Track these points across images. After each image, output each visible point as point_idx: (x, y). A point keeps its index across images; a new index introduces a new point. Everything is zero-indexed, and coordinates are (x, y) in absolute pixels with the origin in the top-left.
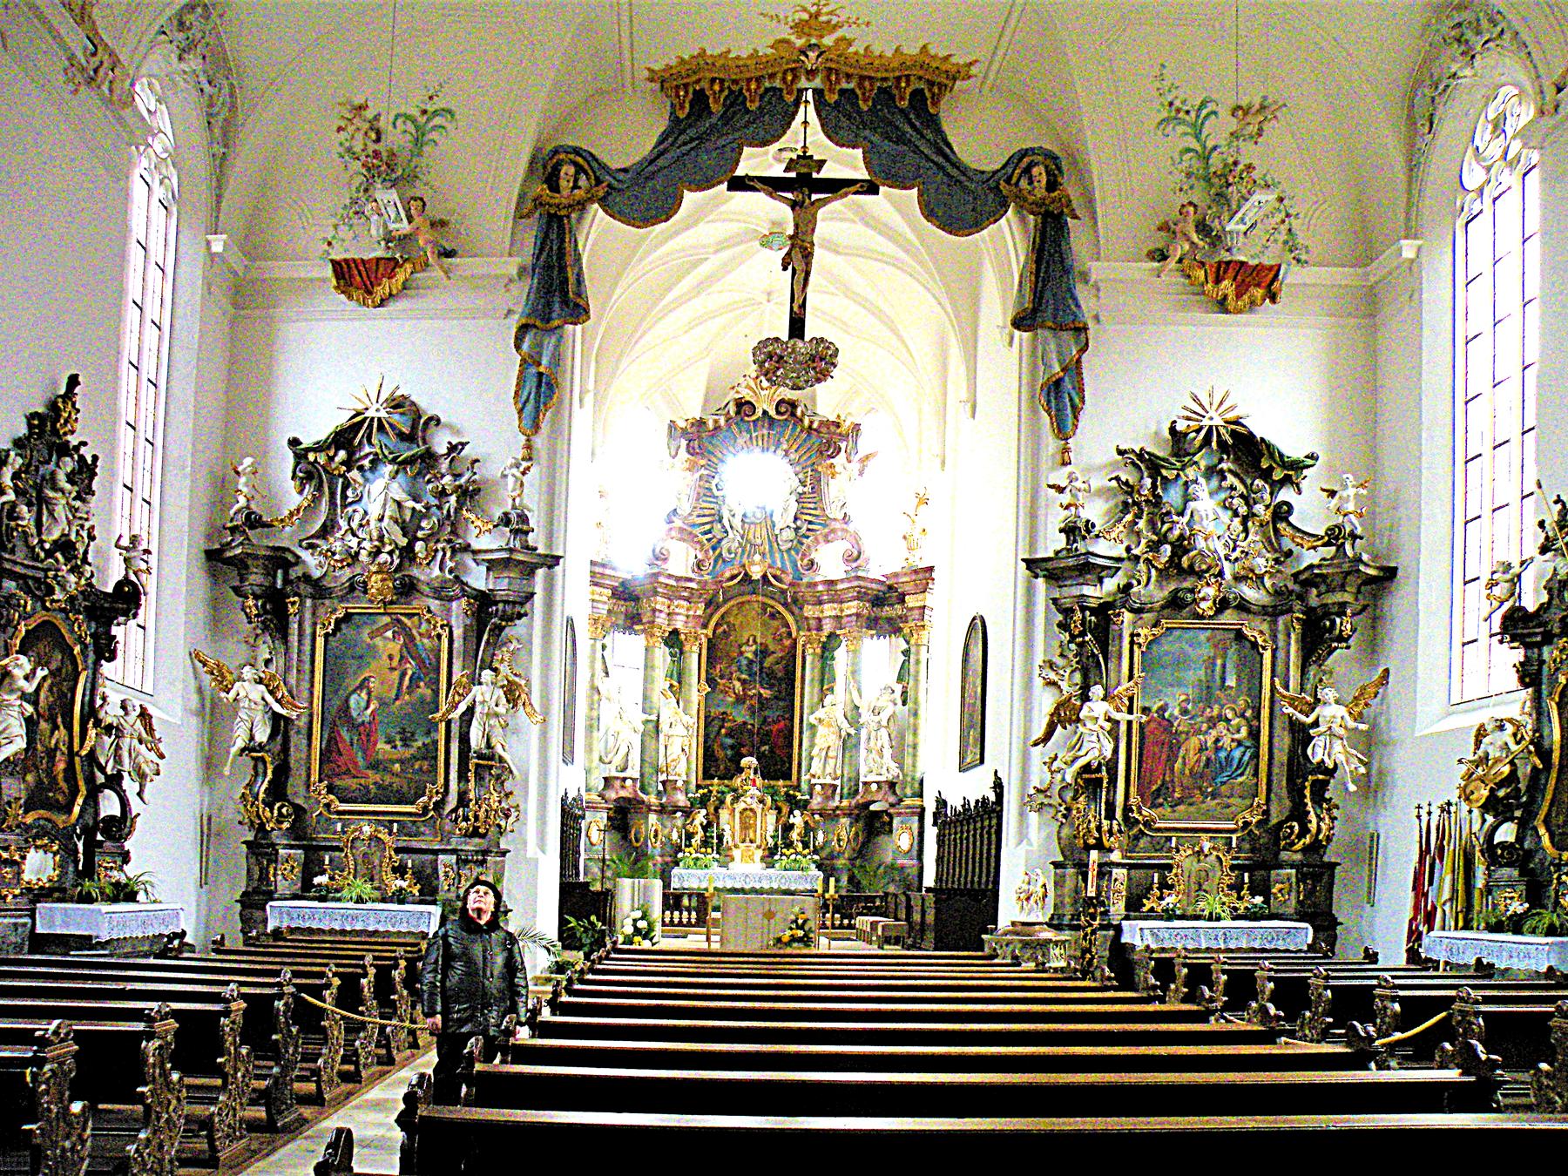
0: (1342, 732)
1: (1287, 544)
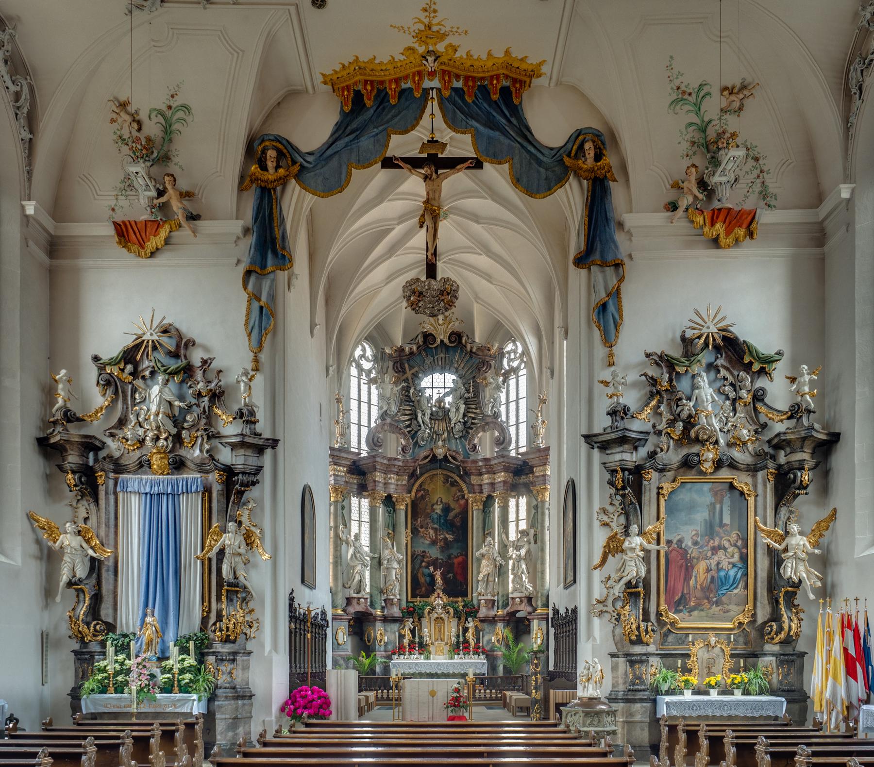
0: (803, 556)
1: (763, 419)
